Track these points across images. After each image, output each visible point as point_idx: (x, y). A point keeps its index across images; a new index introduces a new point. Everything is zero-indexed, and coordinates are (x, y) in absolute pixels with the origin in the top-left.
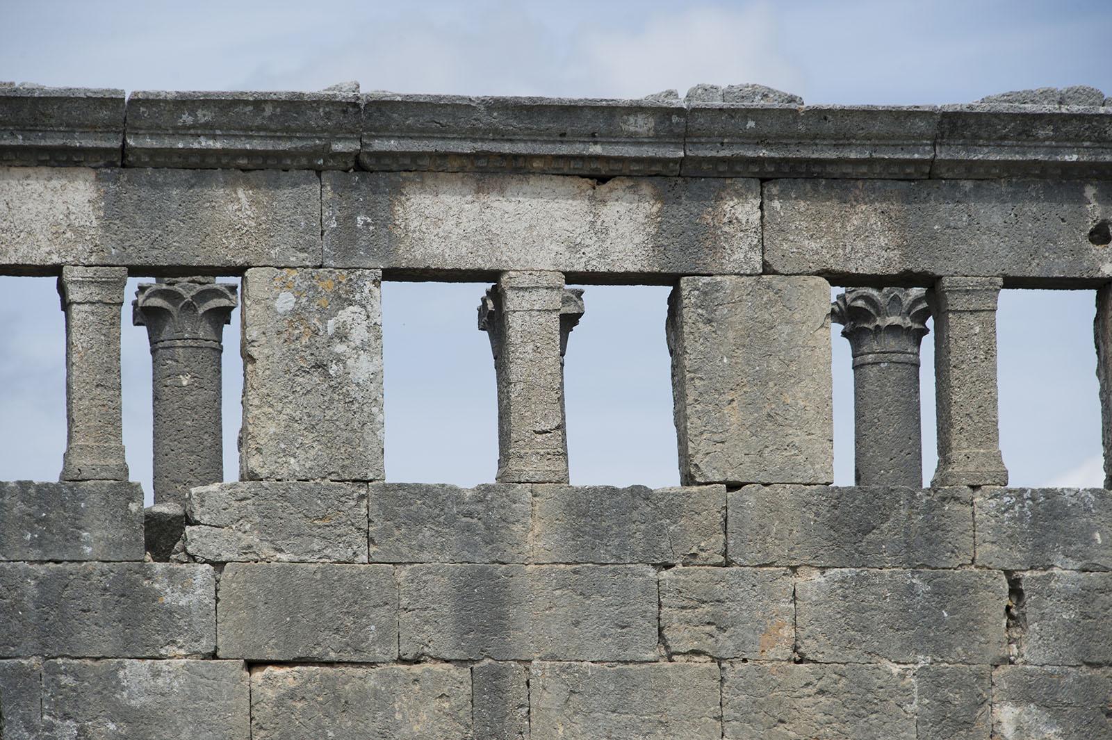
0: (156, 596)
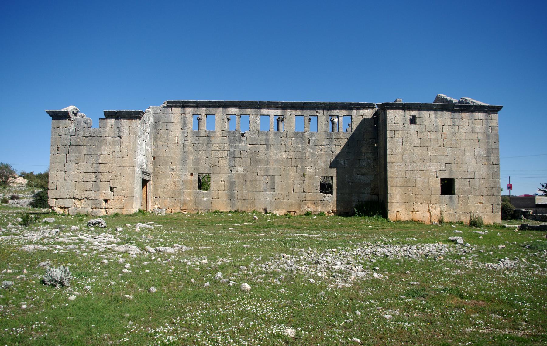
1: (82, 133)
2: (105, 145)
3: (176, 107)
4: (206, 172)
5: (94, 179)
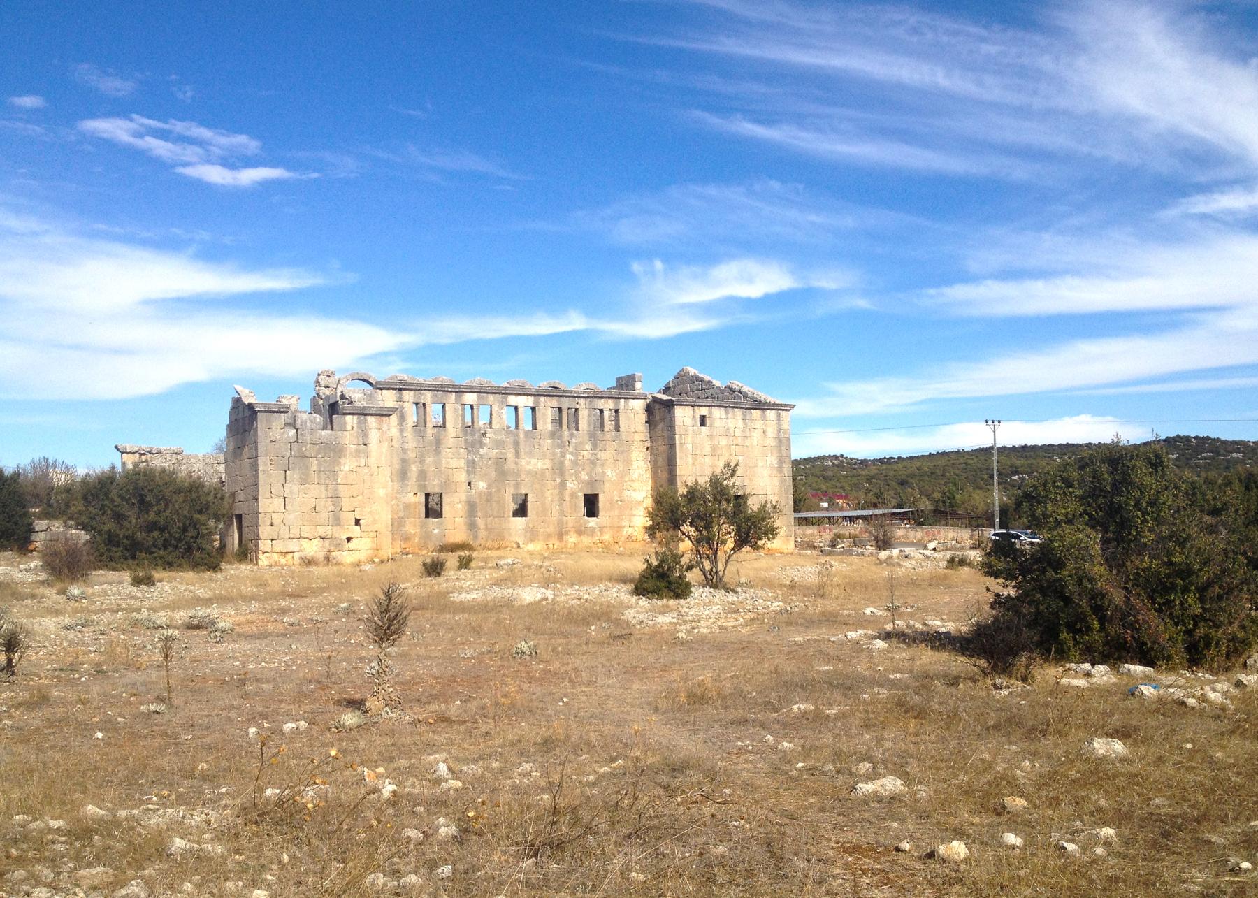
1: (308, 438)
4: (437, 490)
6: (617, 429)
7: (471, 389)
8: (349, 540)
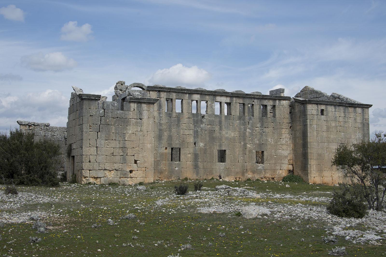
0: (202, 121)
1: (110, 115)
2: (130, 125)
3: (153, 91)
4: (178, 146)
5: (121, 154)
6: (274, 116)
7: (196, 92)
8: (131, 172)
